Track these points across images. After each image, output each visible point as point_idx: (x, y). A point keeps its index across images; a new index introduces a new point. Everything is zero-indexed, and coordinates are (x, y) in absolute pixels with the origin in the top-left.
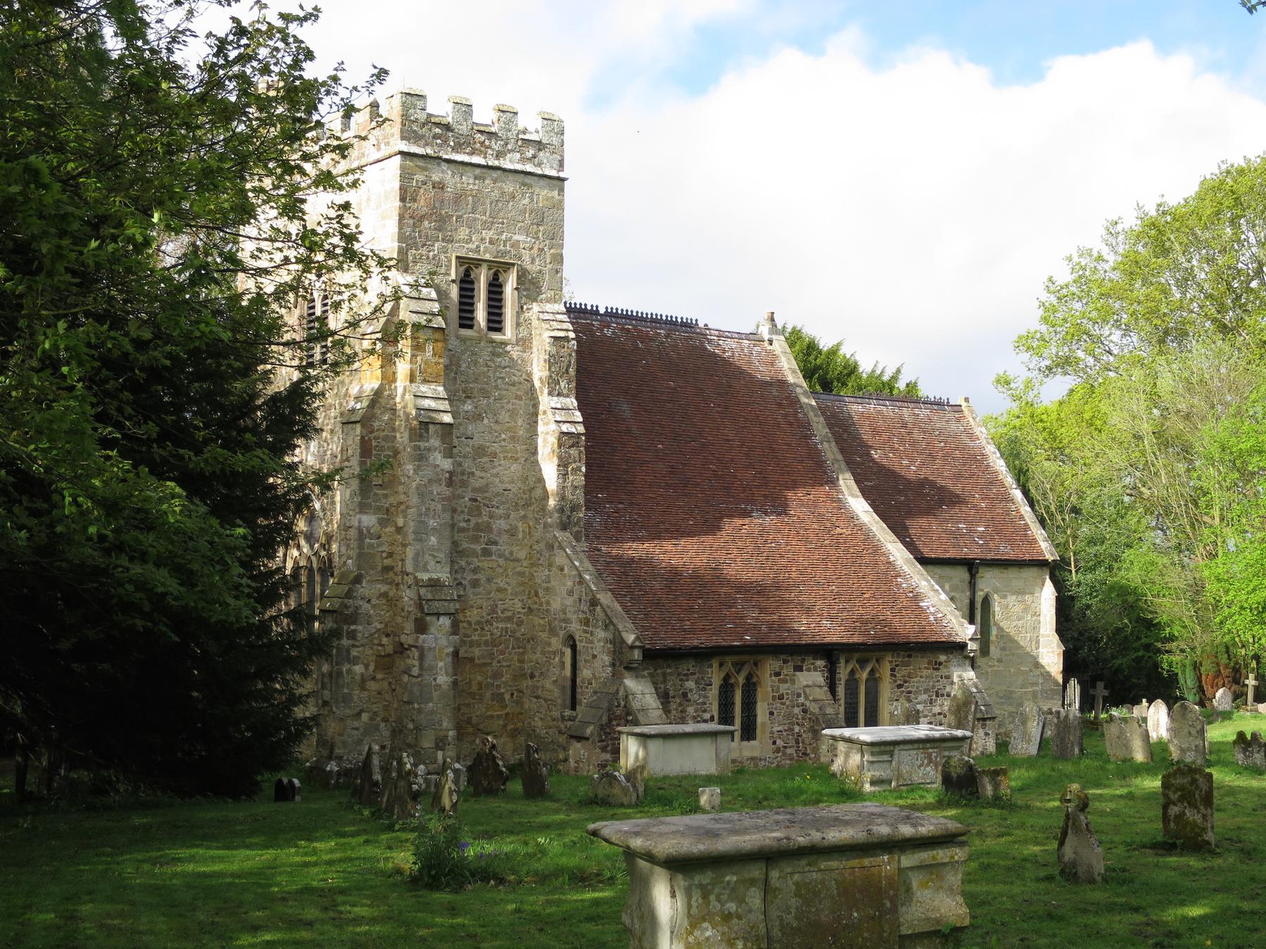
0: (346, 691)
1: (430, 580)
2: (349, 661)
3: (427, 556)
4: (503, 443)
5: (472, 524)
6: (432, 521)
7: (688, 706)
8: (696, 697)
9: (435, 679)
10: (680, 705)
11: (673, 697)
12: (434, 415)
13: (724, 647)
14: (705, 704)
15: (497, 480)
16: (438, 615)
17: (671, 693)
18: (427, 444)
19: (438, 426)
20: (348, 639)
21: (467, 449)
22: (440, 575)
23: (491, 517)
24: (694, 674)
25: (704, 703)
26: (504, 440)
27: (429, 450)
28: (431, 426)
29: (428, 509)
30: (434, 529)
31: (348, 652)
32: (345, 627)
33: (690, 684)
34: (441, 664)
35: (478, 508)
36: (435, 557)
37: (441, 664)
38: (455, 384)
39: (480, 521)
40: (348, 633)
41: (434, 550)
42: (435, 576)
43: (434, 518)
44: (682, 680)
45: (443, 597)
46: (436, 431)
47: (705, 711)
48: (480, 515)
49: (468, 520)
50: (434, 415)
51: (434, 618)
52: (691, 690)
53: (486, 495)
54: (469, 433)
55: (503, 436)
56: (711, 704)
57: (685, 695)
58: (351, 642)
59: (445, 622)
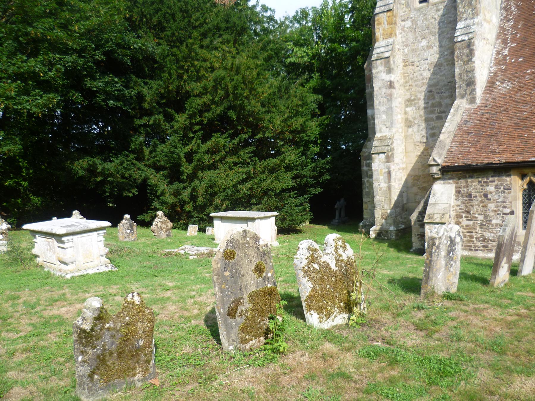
0: (367, 190)
1: (381, 137)
2: (367, 177)
3: (381, 125)
4: (446, 57)
5: (430, 104)
6: (382, 108)
7: (489, 203)
8: (496, 197)
9: (379, 185)
10: (482, 202)
11: (476, 197)
12: (380, 55)
13: (517, 162)
14: (504, 202)
15: (444, 78)
16: (379, 153)
17: (474, 194)
18: (377, 70)
19: (383, 60)
20: (366, 166)
21: (425, 66)
22: (387, 134)
23: (441, 98)
24: (494, 181)
25: (504, 202)
26: (447, 55)
27: (378, 73)
28: (379, 62)
29: (380, 102)
30: (384, 111)
31: (367, 173)
32: (365, 162)
33: (491, 188)
34: (382, 177)
35: (433, 95)
36: (385, 125)
37: (382, 177)
38: (415, 34)
39: (434, 102)
40: (366, 164)
41: (384, 122)
42: (384, 135)
43: (383, 106)
44: (482, 186)
45: (383, 144)
46: (382, 63)
47: (505, 207)
48: (434, 98)
49: (428, 103)
50: (380, 55)
51: (377, 156)
52: (491, 193)
53: (438, 87)
54: (425, 57)
55: (446, 53)
56: (511, 202)
57: (486, 196)
58: (368, 168)
59: (383, 156)
